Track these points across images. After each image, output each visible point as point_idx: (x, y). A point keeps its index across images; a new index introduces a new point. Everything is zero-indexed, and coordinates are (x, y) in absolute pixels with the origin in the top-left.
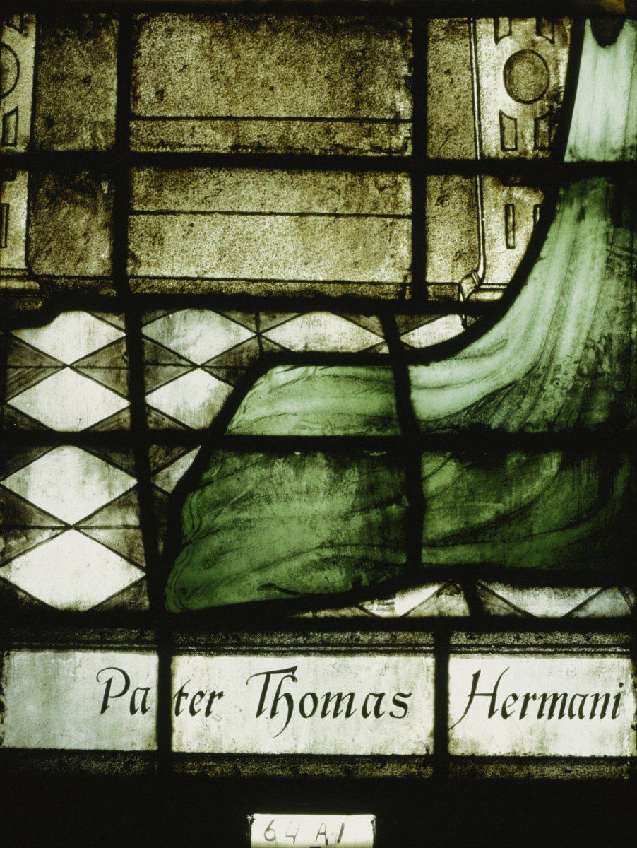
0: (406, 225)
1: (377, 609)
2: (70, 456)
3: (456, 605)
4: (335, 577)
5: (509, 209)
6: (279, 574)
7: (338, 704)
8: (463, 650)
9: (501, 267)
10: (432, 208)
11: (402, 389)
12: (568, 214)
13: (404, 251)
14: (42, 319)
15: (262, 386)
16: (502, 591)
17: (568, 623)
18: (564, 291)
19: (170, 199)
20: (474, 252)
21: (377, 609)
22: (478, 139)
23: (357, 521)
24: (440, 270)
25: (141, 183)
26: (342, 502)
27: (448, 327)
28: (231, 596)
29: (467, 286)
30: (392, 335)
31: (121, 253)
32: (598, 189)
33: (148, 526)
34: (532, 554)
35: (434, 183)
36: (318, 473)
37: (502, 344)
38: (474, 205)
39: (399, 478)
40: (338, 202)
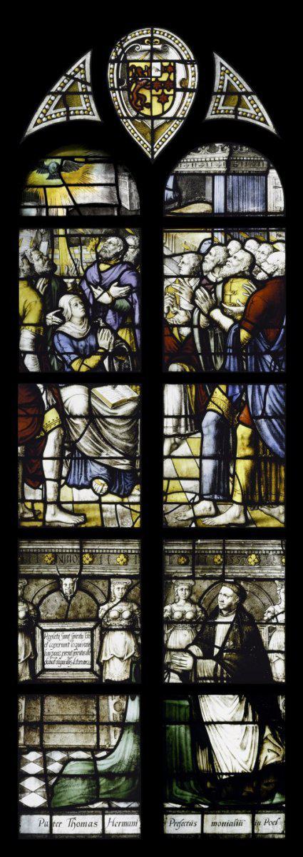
0: (95, 735)
1: (91, 806)
2: (32, 779)
3: (106, 806)
4: (83, 801)
5: (115, 731)
6: (73, 800)
7: (83, 824)
8: (107, 814)
9: (114, 742)
10: (100, 731)
11: (95, 765)
12: (126, 732)
13: (95, 739)
14: (27, 753)
15: (69, 765)
16: (114, 803)
17: (127, 809)
18: (126, 746)
19: (51, 730)
20: (109, 739)
21: (91, 806)
22: (109, 719)
23: (87, 790)
24: (102, 743)
25: (45, 727)
26: (84, 786)
27: (104, 754)
28: (63, 804)
29: (107, 746)
30: (93, 755)
31: (42, 740)
32: (132, 727)
33: (48, 792)
34: (120, 796)
35: (101, 727)
36: (79, 781)
37: (114, 757)
38: (108, 731)
39: (95, 782)
40: (83, 731)
